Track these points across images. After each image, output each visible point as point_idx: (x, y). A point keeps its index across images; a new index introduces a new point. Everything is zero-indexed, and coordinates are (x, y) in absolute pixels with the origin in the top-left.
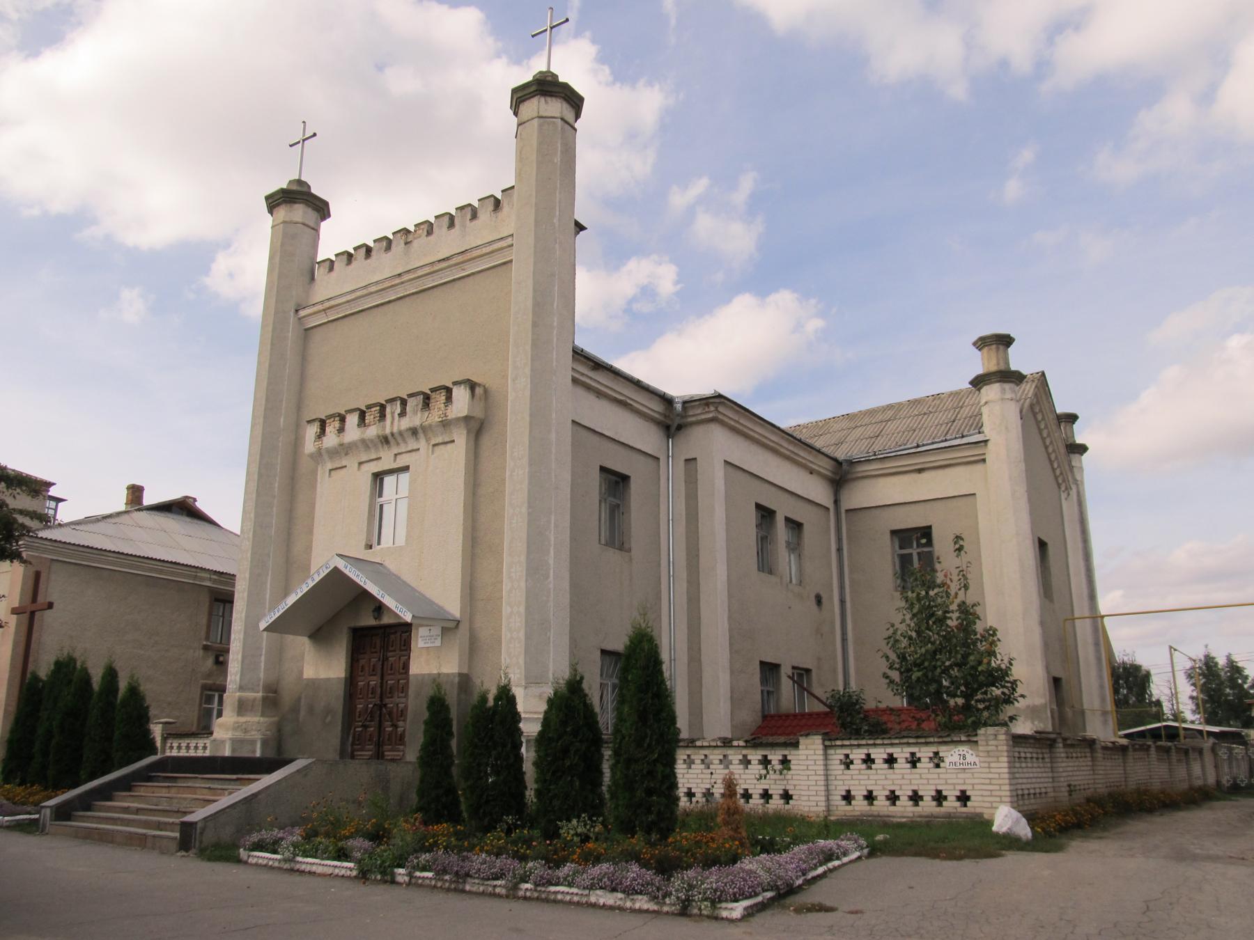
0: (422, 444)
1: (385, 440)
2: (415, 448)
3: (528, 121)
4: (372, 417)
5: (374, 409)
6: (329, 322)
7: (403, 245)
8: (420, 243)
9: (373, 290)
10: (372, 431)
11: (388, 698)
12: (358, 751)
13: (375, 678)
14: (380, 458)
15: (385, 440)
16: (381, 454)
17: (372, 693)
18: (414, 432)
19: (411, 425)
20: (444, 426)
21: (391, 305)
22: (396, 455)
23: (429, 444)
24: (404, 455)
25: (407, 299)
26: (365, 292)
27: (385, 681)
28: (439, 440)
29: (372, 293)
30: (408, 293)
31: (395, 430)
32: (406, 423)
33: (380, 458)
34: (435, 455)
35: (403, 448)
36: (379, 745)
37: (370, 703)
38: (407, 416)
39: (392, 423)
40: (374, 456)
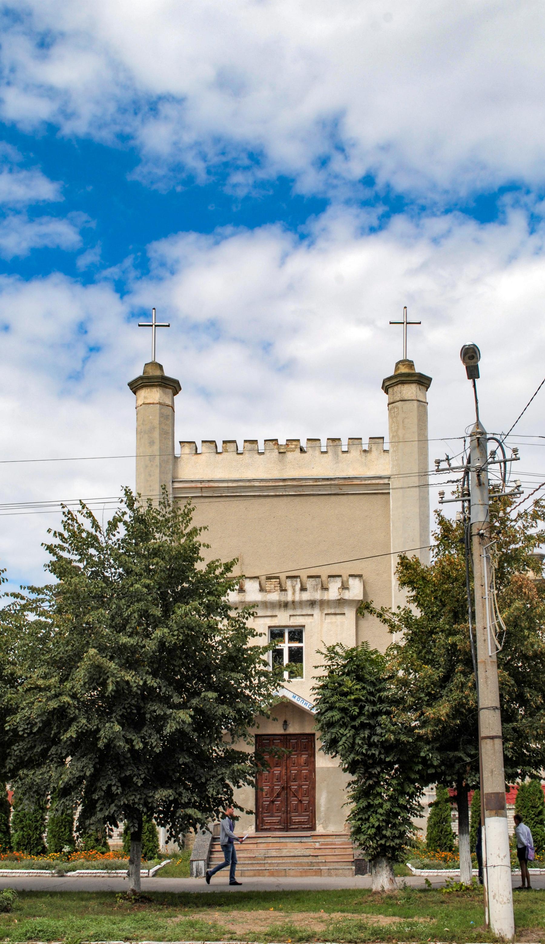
0: (316, 612)
1: (285, 605)
2: (309, 612)
3: (409, 400)
4: (273, 586)
5: (275, 580)
6: (202, 497)
7: (277, 453)
8: (293, 456)
9: (256, 485)
10: (274, 597)
11: (292, 782)
12: (267, 817)
13: (279, 768)
14: (276, 616)
15: (285, 605)
16: (276, 612)
17: (277, 779)
18: (312, 603)
19: (312, 598)
20: (339, 603)
21: (269, 500)
22: (290, 616)
23: (322, 613)
24: (298, 617)
25: (285, 498)
26: (248, 484)
27: (288, 771)
28: (332, 611)
29: (254, 486)
30: (287, 493)
31: (297, 598)
32: (306, 596)
33: (276, 616)
34: (326, 621)
35: (298, 612)
36: (287, 812)
37: (278, 785)
38: (308, 591)
39: (294, 593)
40: (269, 613)
